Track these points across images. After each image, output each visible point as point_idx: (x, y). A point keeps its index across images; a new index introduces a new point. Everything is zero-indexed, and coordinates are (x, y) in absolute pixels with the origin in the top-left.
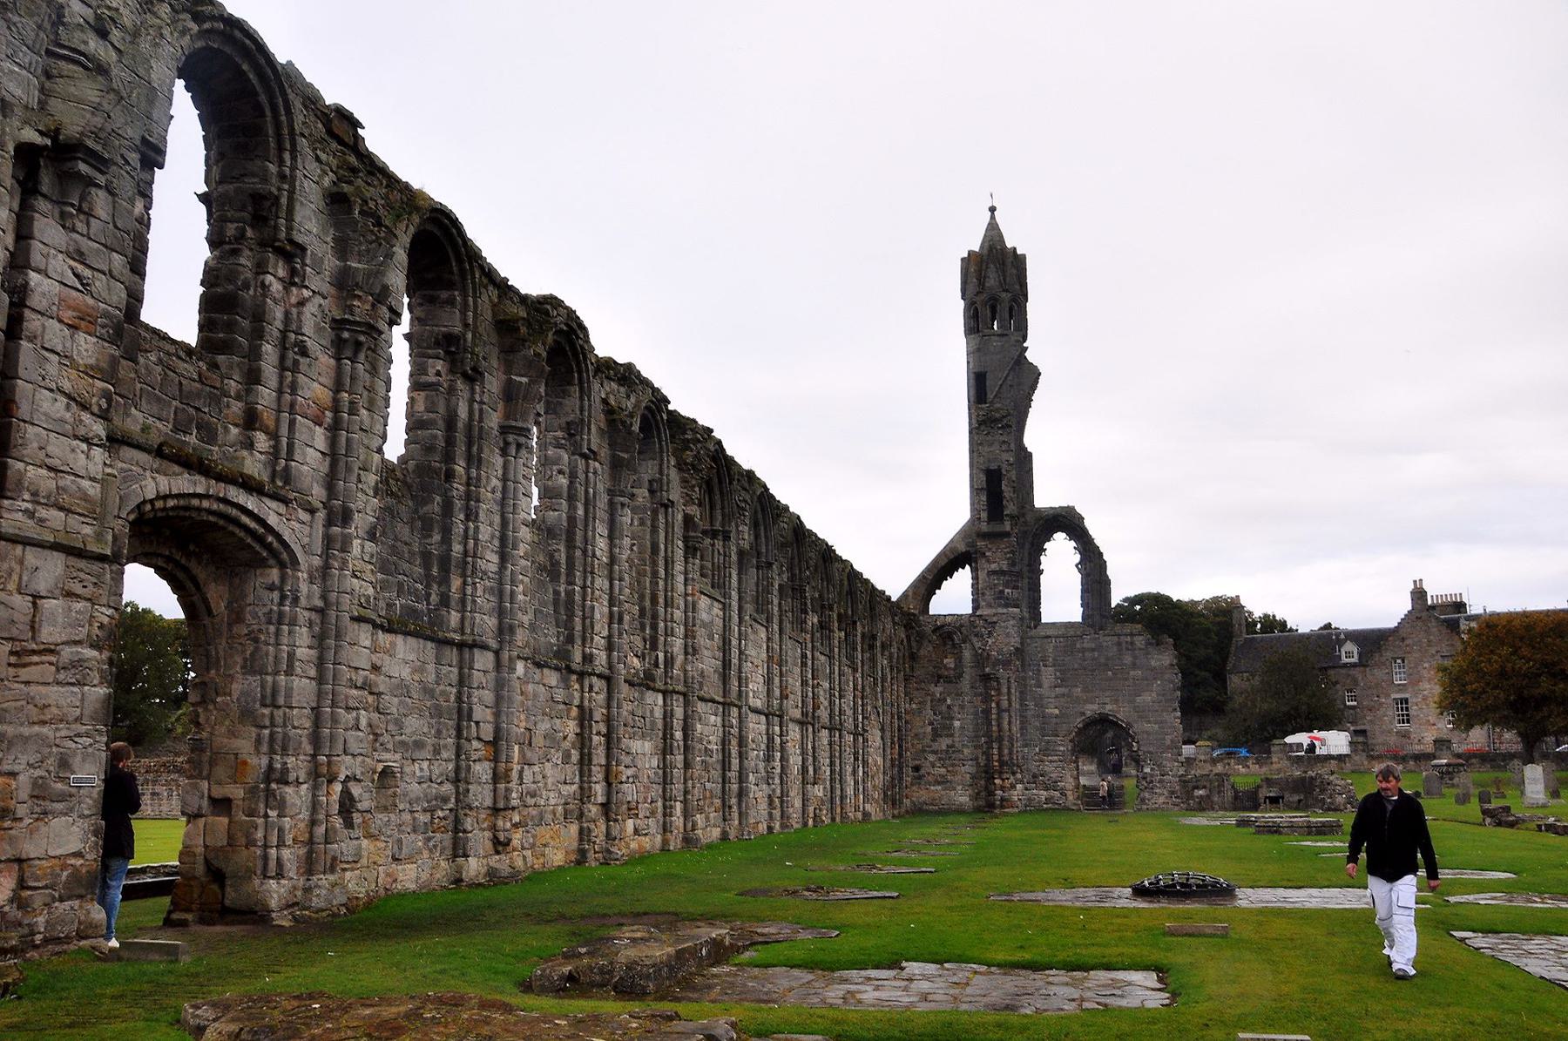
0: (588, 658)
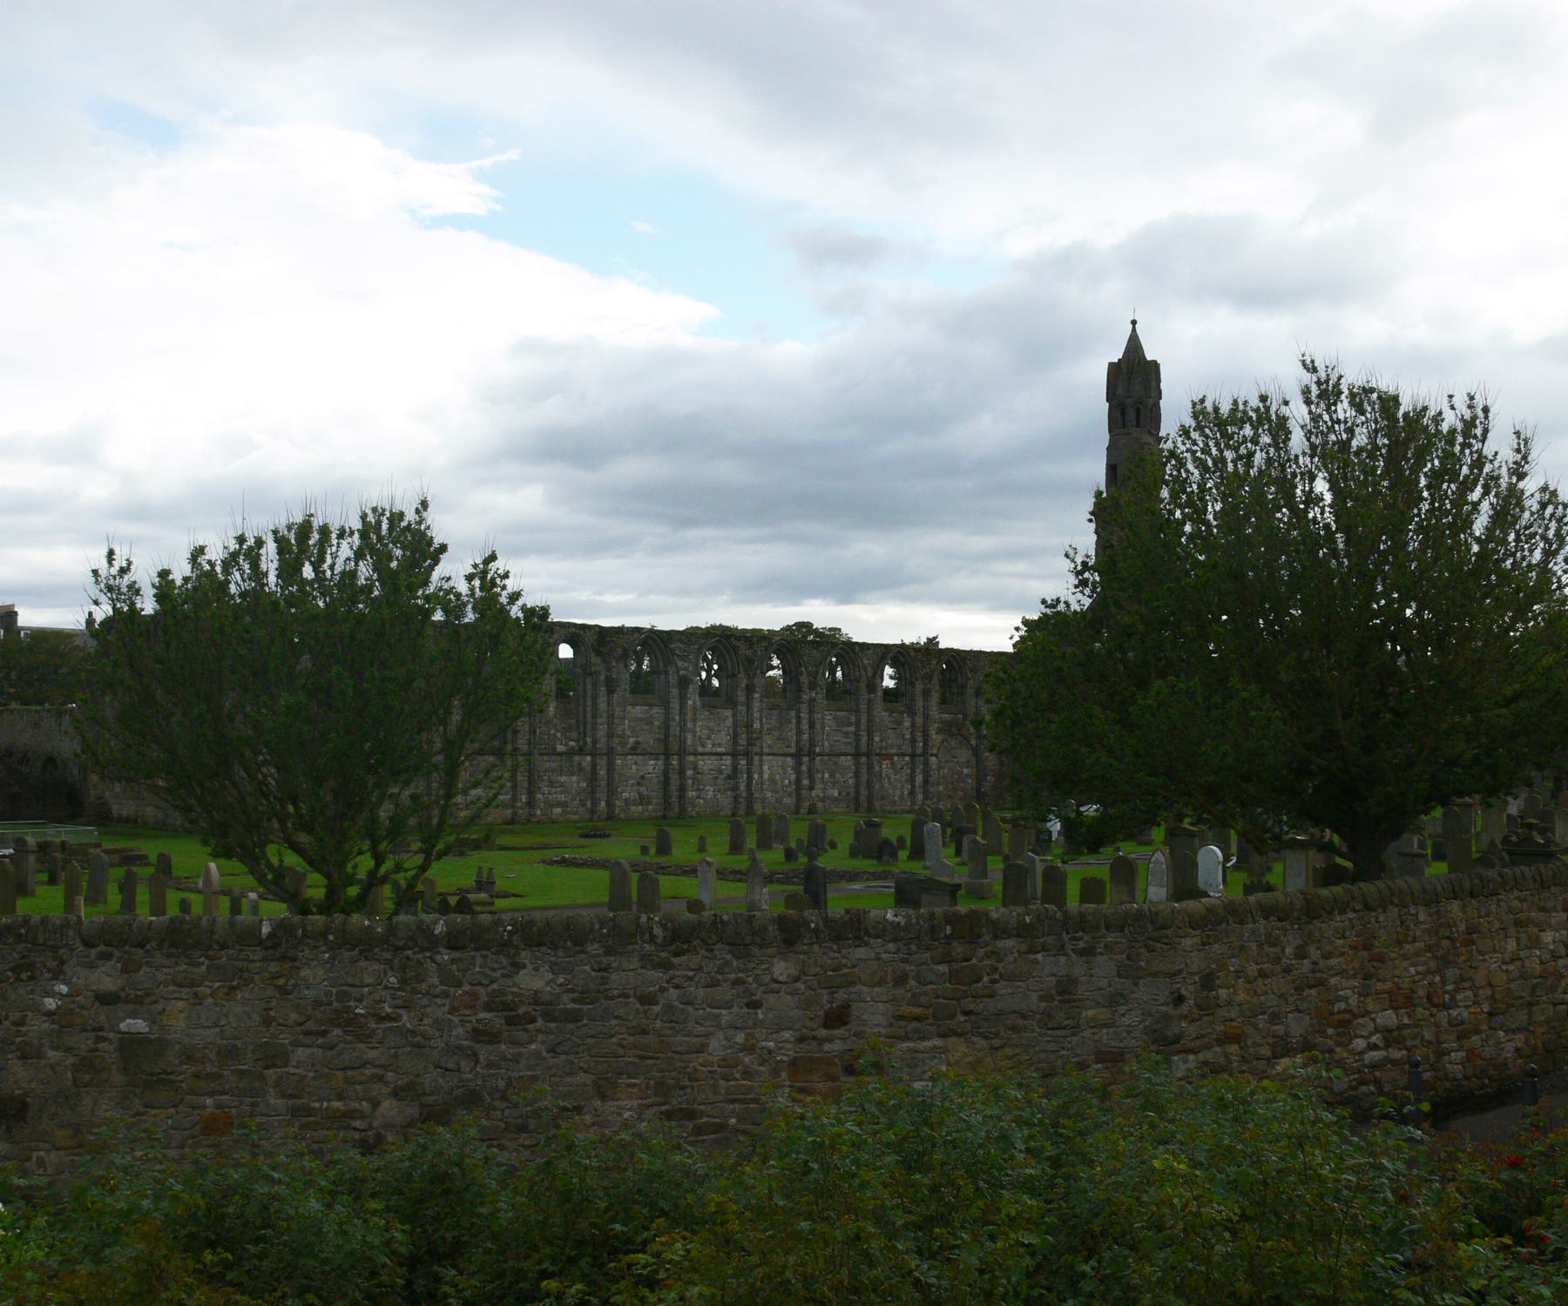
0: (515, 749)
